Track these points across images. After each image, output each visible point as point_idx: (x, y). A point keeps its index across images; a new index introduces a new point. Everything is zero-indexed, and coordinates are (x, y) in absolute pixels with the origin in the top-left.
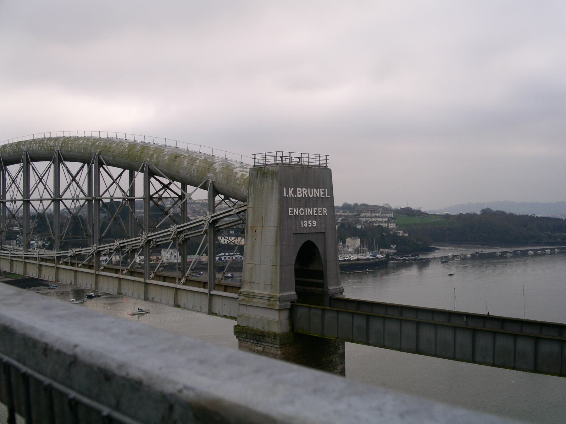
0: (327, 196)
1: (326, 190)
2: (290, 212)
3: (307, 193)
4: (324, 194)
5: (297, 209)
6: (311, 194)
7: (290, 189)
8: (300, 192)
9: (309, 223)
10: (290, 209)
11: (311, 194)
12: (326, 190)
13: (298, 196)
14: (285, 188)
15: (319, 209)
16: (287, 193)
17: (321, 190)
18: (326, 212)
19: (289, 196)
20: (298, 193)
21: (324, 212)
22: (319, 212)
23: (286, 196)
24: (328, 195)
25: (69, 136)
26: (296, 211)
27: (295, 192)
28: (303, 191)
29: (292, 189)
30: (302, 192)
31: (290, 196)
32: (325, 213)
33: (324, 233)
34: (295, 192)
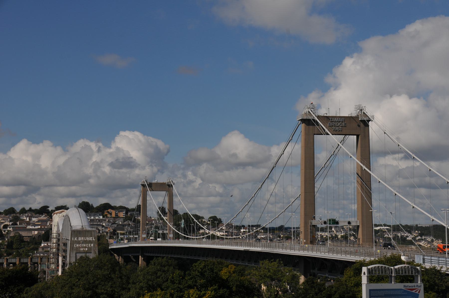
0: (93, 240)
3: (84, 239)
4: (92, 239)
6: (85, 239)
11: (85, 239)
13: (79, 240)
17: (91, 238)
27: (77, 239)
29: (76, 238)
30: (81, 239)
34: (77, 239)
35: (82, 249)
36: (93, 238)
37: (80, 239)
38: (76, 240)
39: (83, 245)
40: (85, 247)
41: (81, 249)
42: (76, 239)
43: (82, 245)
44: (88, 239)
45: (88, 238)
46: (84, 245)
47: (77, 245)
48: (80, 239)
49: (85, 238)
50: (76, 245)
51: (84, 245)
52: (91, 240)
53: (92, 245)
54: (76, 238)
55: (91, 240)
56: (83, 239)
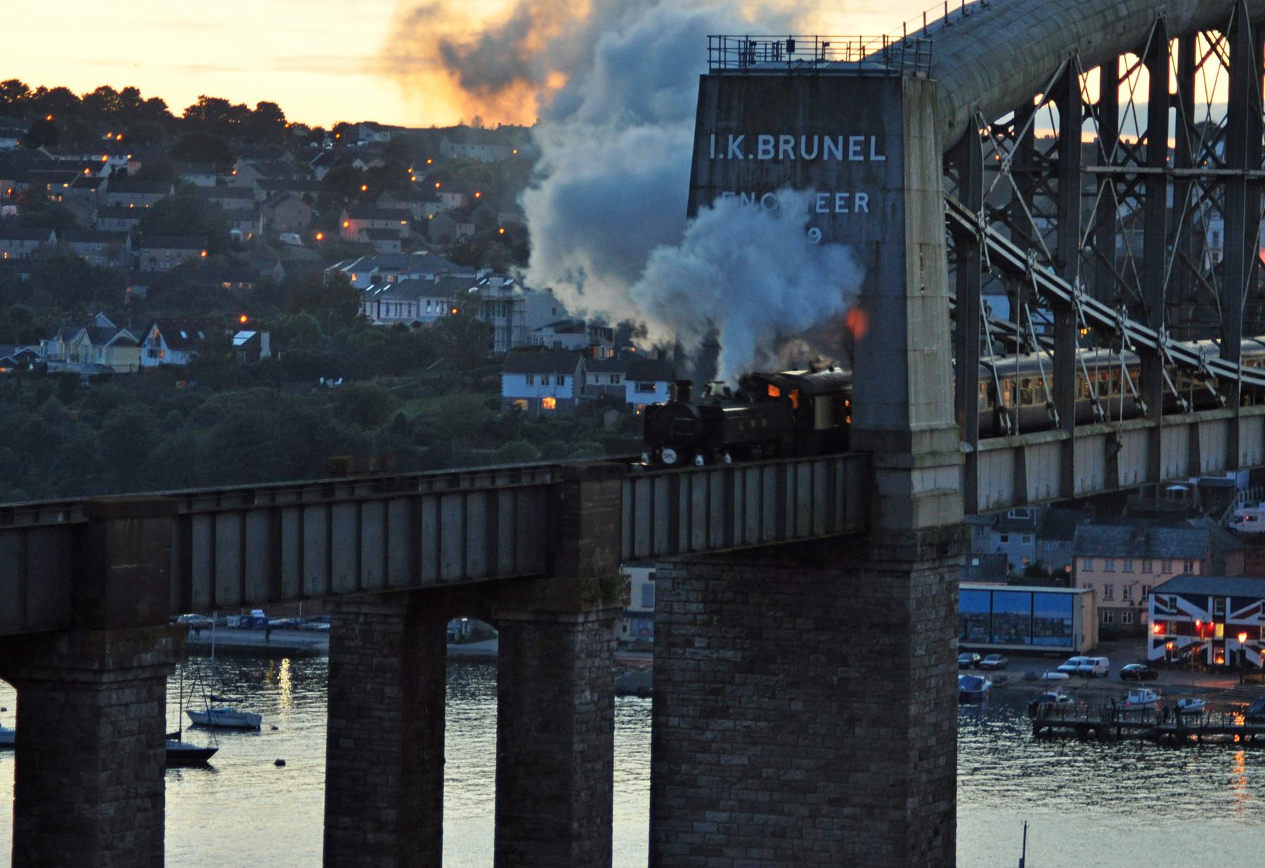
1: (873, 139)
3: (796, 149)
4: (866, 151)
6: (809, 151)
7: (731, 137)
8: (770, 147)
11: (809, 151)
12: (873, 139)
13: (760, 156)
15: (838, 195)
16: (722, 147)
17: (852, 139)
18: (864, 203)
19: (726, 154)
20: (761, 147)
21: (857, 202)
22: (838, 203)
23: (716, 154)
24: (877, 153)
29: (741, 137)
30: (776, 147)
36: (866, 146)
38: (741, 157)
42: (734, 146)
44: (832, 149)
48: (766, 152)
52: (852, 157)
53: (861, 200)
54: (741, 137)
56: (789, 147)
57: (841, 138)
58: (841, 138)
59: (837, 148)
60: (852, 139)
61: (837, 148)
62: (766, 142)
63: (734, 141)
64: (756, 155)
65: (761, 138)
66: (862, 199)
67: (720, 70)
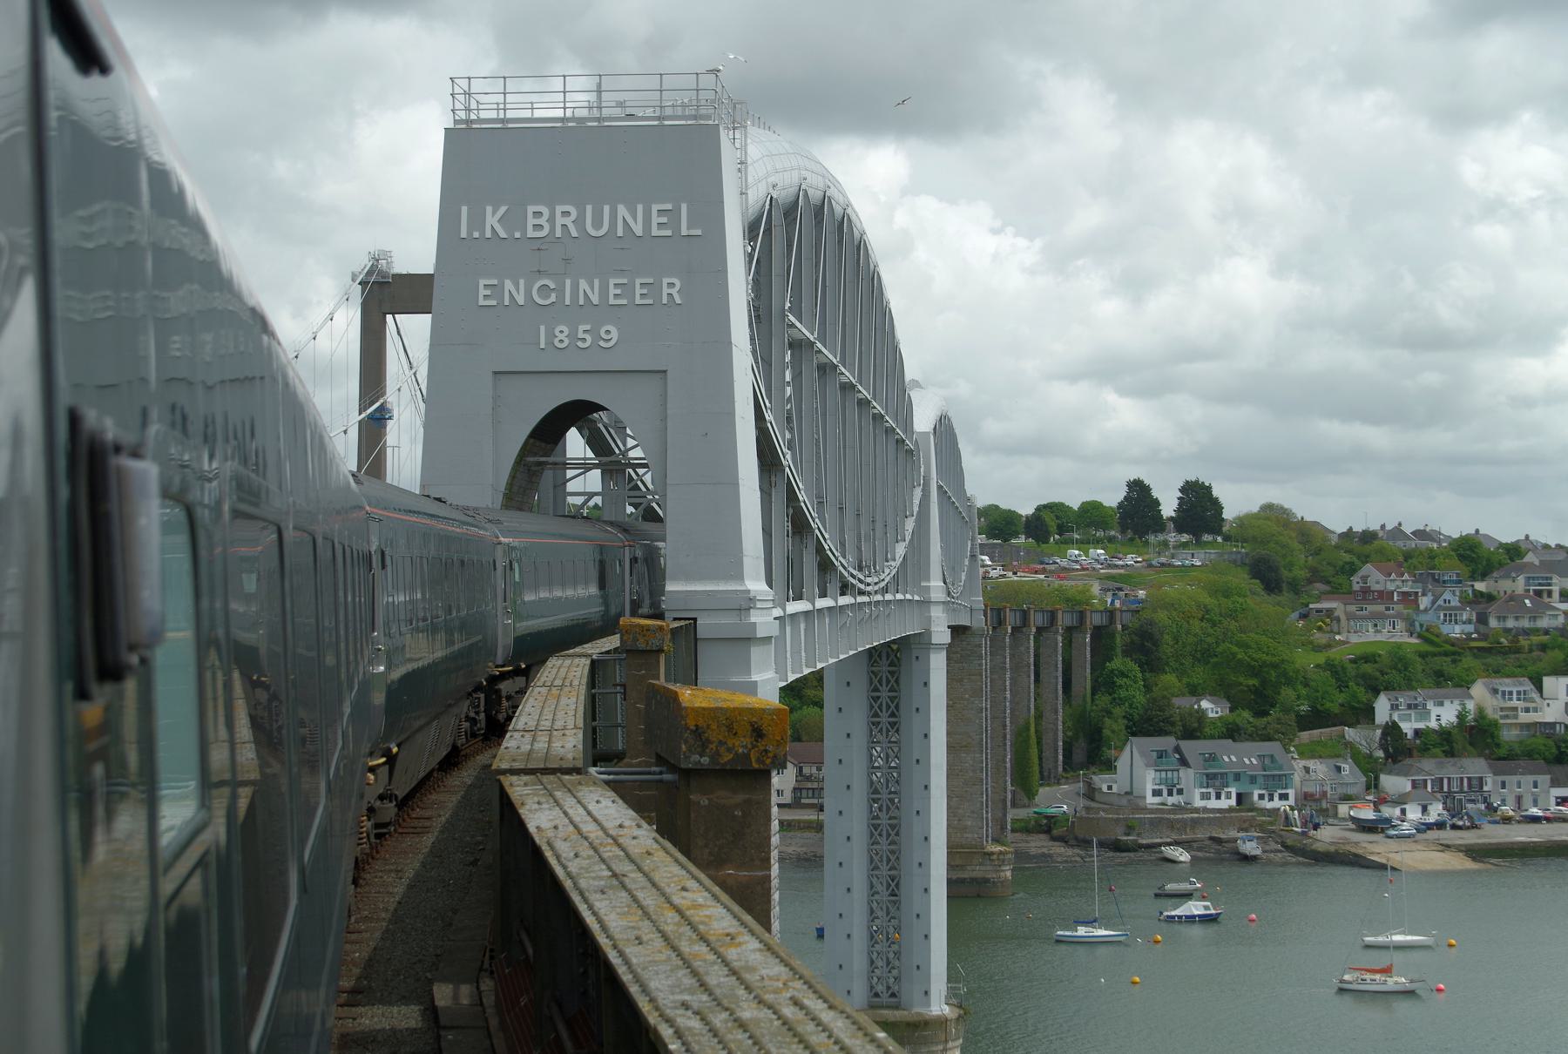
0: (684, 232)
1: (684, 207)
2: (483, 292)
3: (580, 222)
5: (522, 282)
6: (598, 223)
7: (489, 209)
8: (542, 221)
9: (581, 335)
10: (482, 282)
11: (598, 223)
12: (684, 207)
13: (531, 233)
14: (464, 209)
15: (638, 281)
16: (477, 221)
19: (483, 232)
20: (531, 221)
21: (666, 291)
22: (638, 291)
23: (470, 233)
25: (595, 93)
26: (592, 289)
28: (558, 214)
29: (503, 209)
30: (552, 220)
31: (488, 234)
32: (670, 295)
33: (665, 372)
35: (562, 332)
36: (674, 214)
37: (540, 227)
38: (503, 234)
39: (575, 287)
40: (598, 312)
41: (551, 335)
42: (492, 219)
43: (560, 291)
45: (622, 211)
46: (589, 290)
47: (508, 285)
48: (538, 227)
49: (589, 208)
50: (497, 290)
51: (589, 290)
55: (655, 232)
56: (568, 221)
57: (640, 208)
58: (640, 208)
59: (635, 219)
60: (655, 208)
61: (635, 219)
62: (538, 214)
63: (494, 213)
64: (524, 231)
65: (531, 209)
66: (671, 285)
67: (468, 121)
